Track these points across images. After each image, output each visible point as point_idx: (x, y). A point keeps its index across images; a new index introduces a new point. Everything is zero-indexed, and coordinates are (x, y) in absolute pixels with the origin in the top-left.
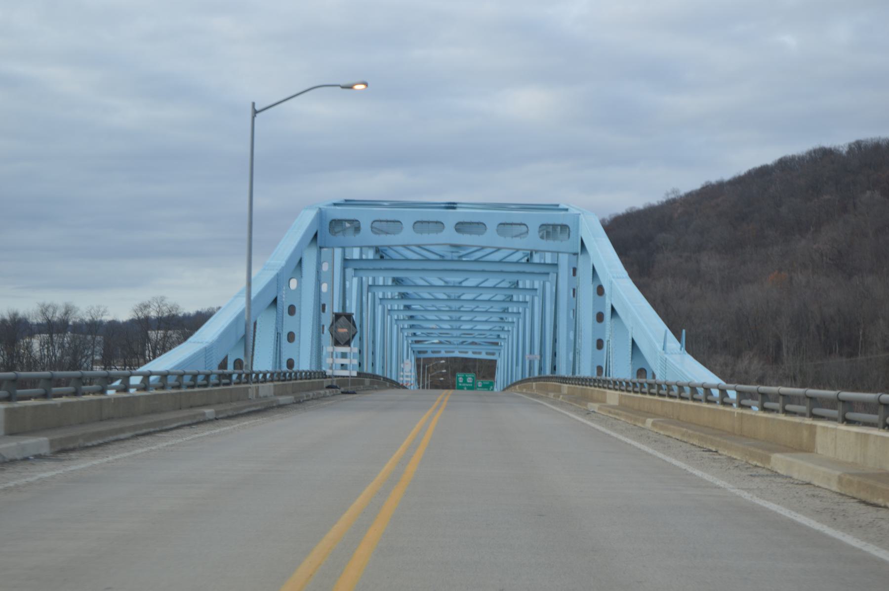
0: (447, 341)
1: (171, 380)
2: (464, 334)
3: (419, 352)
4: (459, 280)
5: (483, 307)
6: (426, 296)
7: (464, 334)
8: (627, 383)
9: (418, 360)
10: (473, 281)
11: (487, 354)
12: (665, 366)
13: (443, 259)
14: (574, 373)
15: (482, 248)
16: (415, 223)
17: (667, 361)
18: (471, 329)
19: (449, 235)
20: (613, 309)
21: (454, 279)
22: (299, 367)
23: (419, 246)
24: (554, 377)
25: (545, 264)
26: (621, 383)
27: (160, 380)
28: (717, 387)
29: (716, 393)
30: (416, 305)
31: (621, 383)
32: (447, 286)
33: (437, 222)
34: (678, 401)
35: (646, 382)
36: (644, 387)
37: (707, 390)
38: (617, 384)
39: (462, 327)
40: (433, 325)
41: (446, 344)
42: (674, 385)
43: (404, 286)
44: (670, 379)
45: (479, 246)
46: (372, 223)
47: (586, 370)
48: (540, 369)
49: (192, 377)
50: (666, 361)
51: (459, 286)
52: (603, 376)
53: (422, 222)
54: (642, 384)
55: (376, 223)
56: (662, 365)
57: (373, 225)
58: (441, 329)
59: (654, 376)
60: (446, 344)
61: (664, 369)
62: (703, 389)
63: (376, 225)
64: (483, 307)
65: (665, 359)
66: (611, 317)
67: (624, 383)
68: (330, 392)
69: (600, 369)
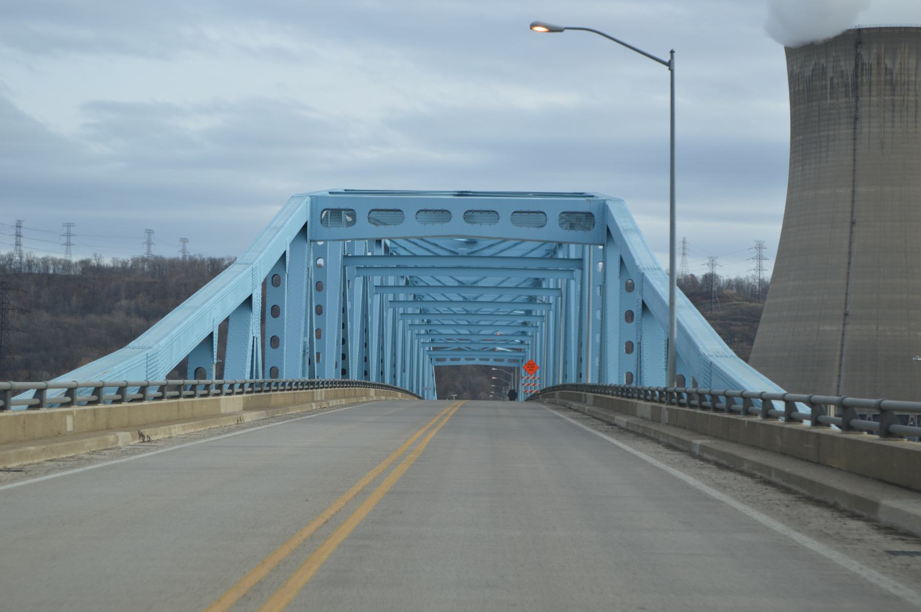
0: (468, 348)
1: (132, 392)
2: (484, 340)
3: (438, 360)
4: (474, 279)
5: (505, 309)
6: (440, 298)
7: (484, 340)
8: (661, 393)
9: (437, 369)
10: (491, 280)
11: (495, 360)
12: (709, 371)
13: (455, 255)
14: (312, 375)
15: (505, 240)
16: (418, 212)
17: (712, 366)
18: (491, 335)
19: (458, 226)
20: (644, 306)
21: (467, 278)
22: (352, 378)
23: (422, 239)
24: (346, 383)
25: (569, 259)
26: (653, 392)
27: (118, 393)
28: (782, 398)
29: (779, 406)
30: (431, 308)
31: (653, 392)
32: (462, 285)
33: (443, 211)
34: (710, 413)
35: (685, 392)
36: (694, 399)
37: (767, 400)
38: (673, 397)
39: (481, 333)
40: (451, 331)
41: (466, 350)
42: (707, 394)
43: (226, 267)
44: (718, 388)
45: (502, 238)
46: (370, 213)
47: (614, 378)
48: (565, 377)
49: (68, 390)
50: (710, 366)
51: (473, 286)
52: (633, 385)
53: (426, 211)
54: (679, 394)
55: (373, 212)
56: (706, 370)
57: (370, 216)
58: (459, 334)
59: (695, 384)
60: (466, 350)
61: (708, 374)
62: (761, 401)
63: (374, 214)
64: (505, 309)
65: (710, 364)
66: (642, 316)
67: (657, 393)
68: (316, 405)
69: (630, 377)
